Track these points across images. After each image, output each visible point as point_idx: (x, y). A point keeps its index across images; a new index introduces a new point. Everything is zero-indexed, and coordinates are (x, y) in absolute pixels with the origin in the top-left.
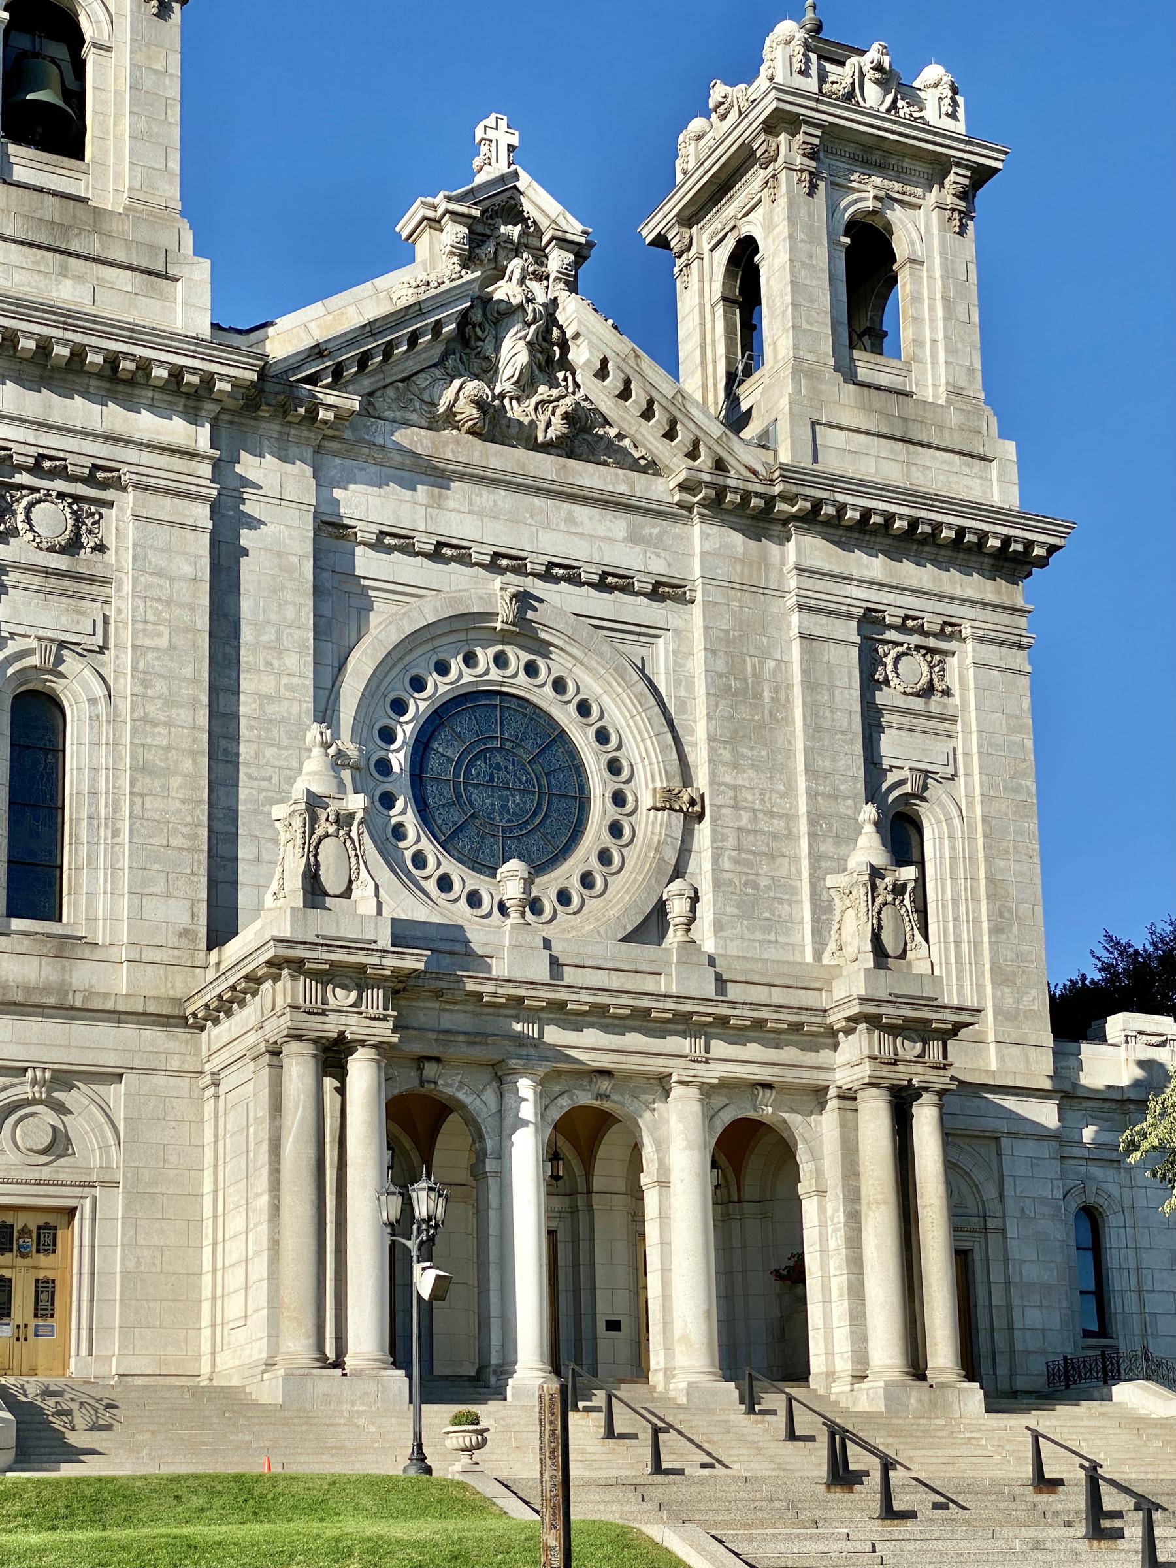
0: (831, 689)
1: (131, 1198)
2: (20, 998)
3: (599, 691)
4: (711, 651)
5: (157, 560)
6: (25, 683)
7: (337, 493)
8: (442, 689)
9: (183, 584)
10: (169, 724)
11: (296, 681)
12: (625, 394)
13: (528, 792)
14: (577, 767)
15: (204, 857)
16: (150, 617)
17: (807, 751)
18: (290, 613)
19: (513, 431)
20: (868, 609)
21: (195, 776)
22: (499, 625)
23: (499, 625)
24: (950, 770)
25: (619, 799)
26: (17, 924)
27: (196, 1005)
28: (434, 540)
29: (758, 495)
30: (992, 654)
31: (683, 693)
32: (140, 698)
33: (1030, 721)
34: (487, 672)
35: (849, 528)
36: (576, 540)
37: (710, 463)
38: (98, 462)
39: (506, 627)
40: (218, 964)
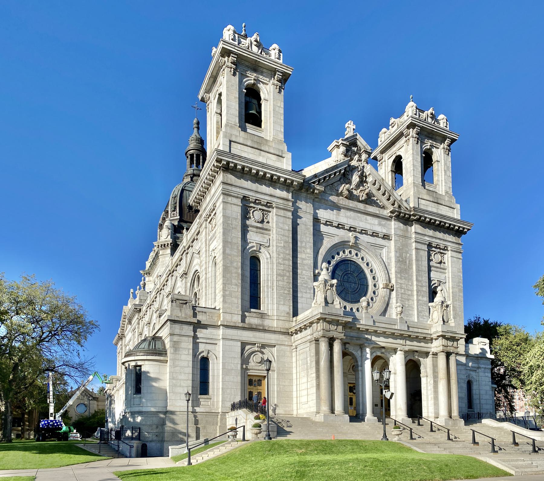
0: (422, 261)
1: (278, 374)
2: (255, 327)
3: (371, 260)
4: (396, 251)
5: (281, 225)
6: (253, 254)
7: (317, 211)
9: (286, 231)
10: (284, 264)
11: (309, 255)
12: (379, 189)
14: (365, 278)
15: (291, 296)
16: (280, 239)
17: (417, 276)
18: (308, 239)
19: (355, 197)
20: (429, 243)
21: (289, 277)
22: (351, 244)
23: (351, 244)
24: (445, 281)
25: (375, 286)
26: (252, 310)
27: (293, 330)
29: (408, 214)
30: (455, 254)
31: (389, 261)
32: (278, 258)
33: (462, 270)
34: (348, 255)
35: (426, 223)
36: (367, 224)
37: (397, 206)
38: (268, 201)
40: (296, 321)
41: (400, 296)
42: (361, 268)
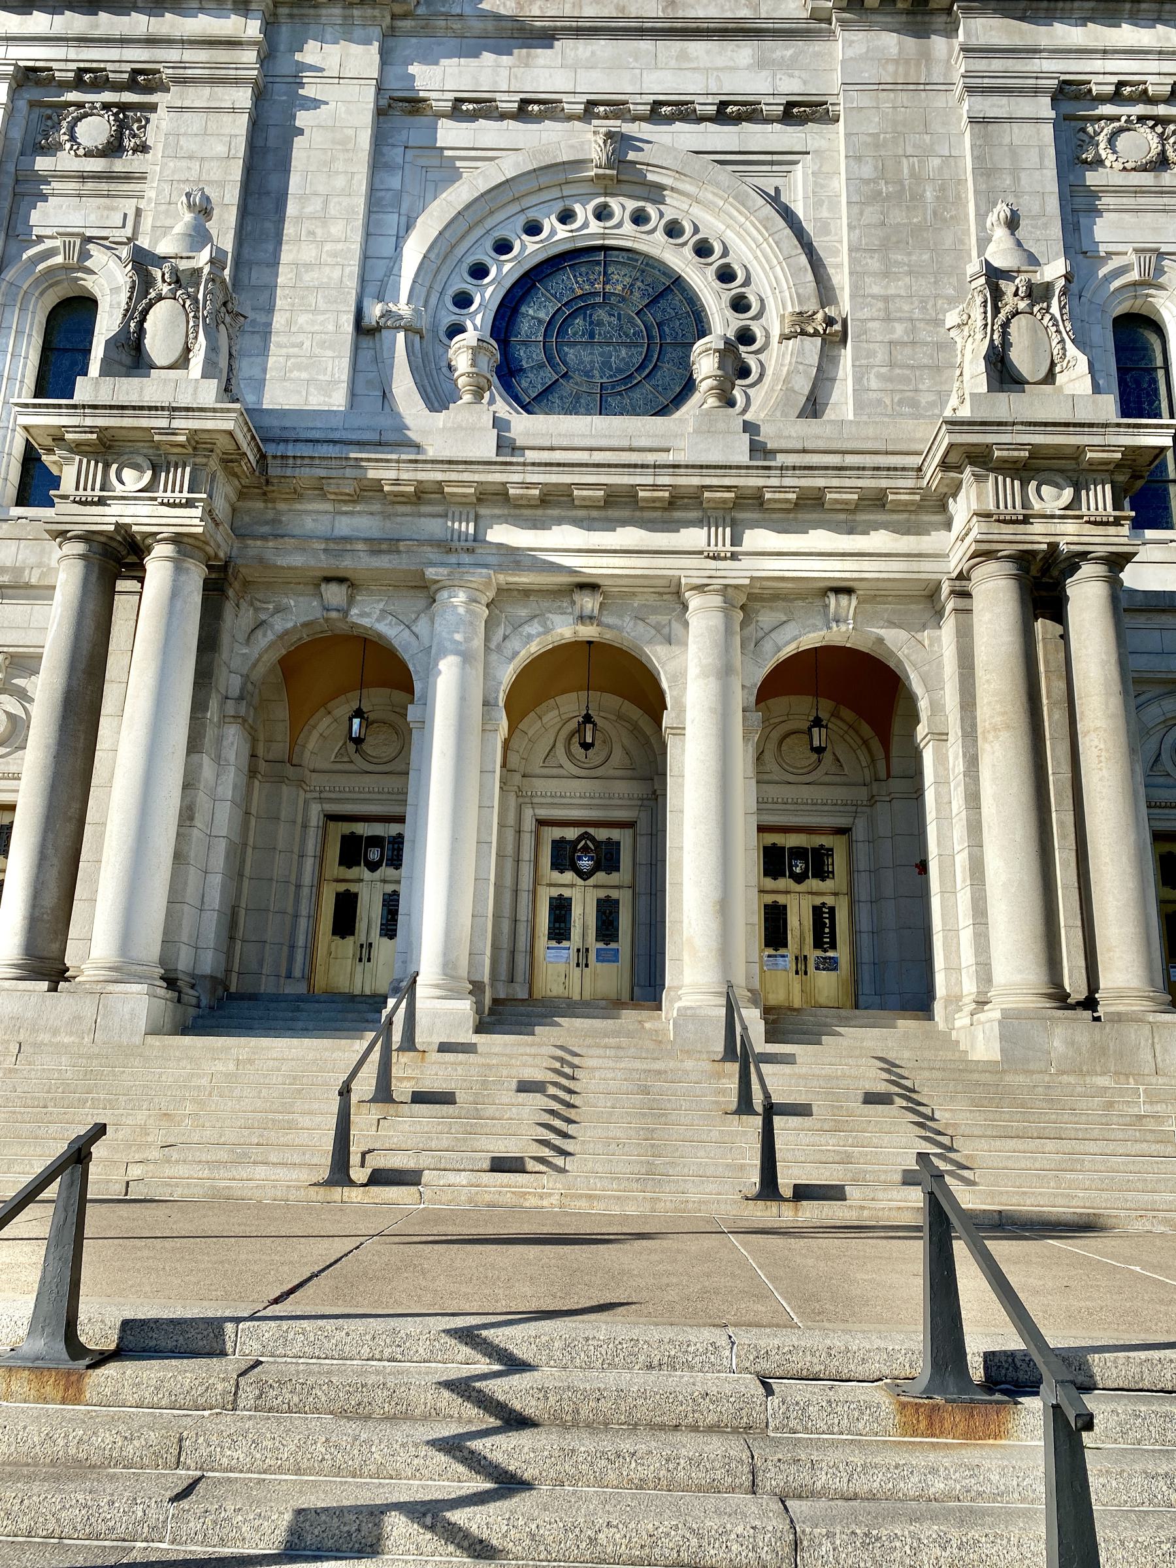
8: (531, 248)
13: (636, 345)
20: (1065, 82)
28: (517, 97)
36: (689, 74)
39: (601, 171)
41: (881, 356)
42: (666, 270)
